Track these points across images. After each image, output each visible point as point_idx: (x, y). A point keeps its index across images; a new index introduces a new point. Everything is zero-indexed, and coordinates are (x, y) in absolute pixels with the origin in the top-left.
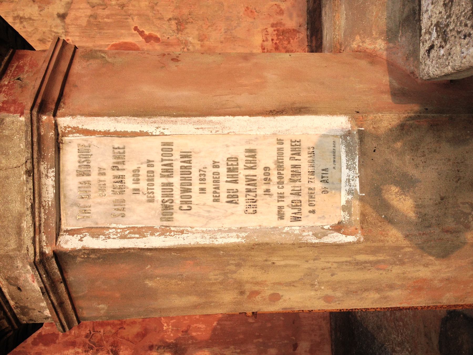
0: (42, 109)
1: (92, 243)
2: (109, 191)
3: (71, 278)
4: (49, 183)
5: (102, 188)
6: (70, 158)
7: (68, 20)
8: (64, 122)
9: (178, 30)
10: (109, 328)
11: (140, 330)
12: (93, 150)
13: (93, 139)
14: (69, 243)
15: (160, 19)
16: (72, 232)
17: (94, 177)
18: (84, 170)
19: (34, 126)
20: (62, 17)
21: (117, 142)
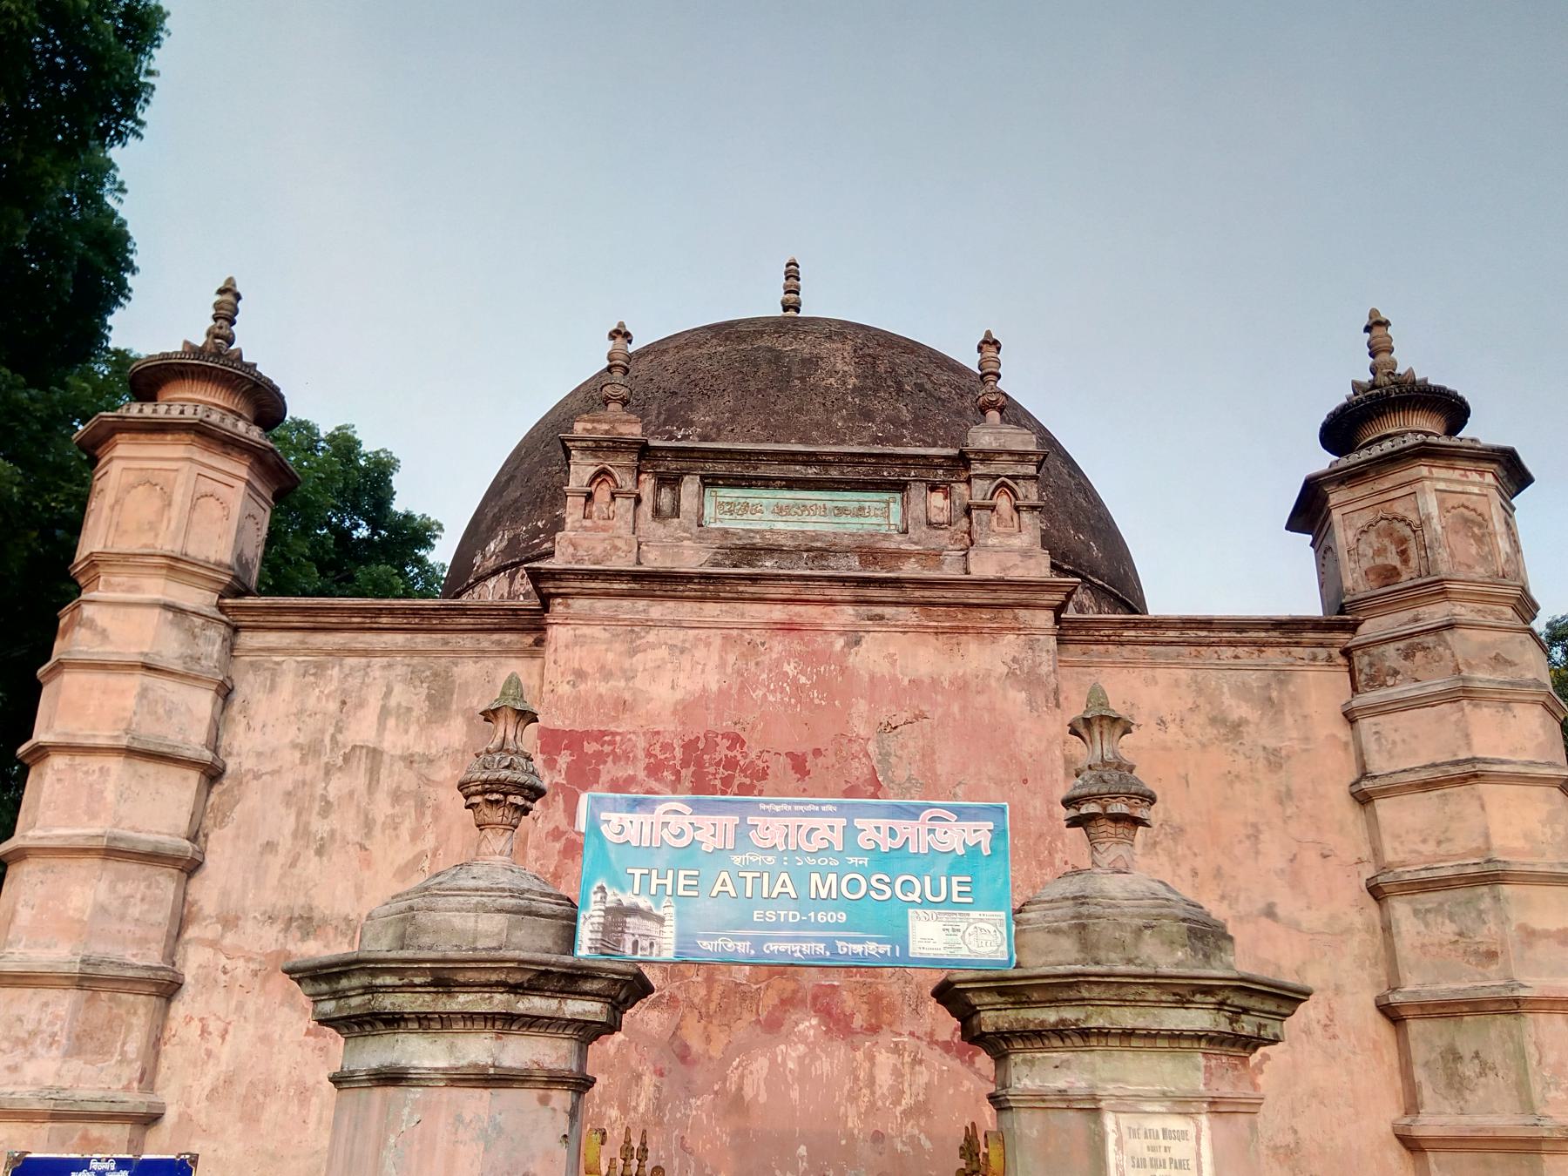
0: (1211, 1103)
1: (1111, 1139)
2: (1152, 1155)
3: (1070, 1113)
4: (1156, 1107)
5: (1152, 1149)
6: (1176, 1123)
7: (1265, 922)
8: (1204, 1120)
9: (1276, 1148)
10: (703, 992)
11: (694, 1050)
12: (1184, 1142)
13: (1193, 1143)
14: (1109, 1121)
15: (1293, 1109)
16: (1117, 1124)
17: (1163, 1143)
18: (1166, 1133)
19: (1200, 1098)
20: (1270, 912)
21: (1193, 1163)
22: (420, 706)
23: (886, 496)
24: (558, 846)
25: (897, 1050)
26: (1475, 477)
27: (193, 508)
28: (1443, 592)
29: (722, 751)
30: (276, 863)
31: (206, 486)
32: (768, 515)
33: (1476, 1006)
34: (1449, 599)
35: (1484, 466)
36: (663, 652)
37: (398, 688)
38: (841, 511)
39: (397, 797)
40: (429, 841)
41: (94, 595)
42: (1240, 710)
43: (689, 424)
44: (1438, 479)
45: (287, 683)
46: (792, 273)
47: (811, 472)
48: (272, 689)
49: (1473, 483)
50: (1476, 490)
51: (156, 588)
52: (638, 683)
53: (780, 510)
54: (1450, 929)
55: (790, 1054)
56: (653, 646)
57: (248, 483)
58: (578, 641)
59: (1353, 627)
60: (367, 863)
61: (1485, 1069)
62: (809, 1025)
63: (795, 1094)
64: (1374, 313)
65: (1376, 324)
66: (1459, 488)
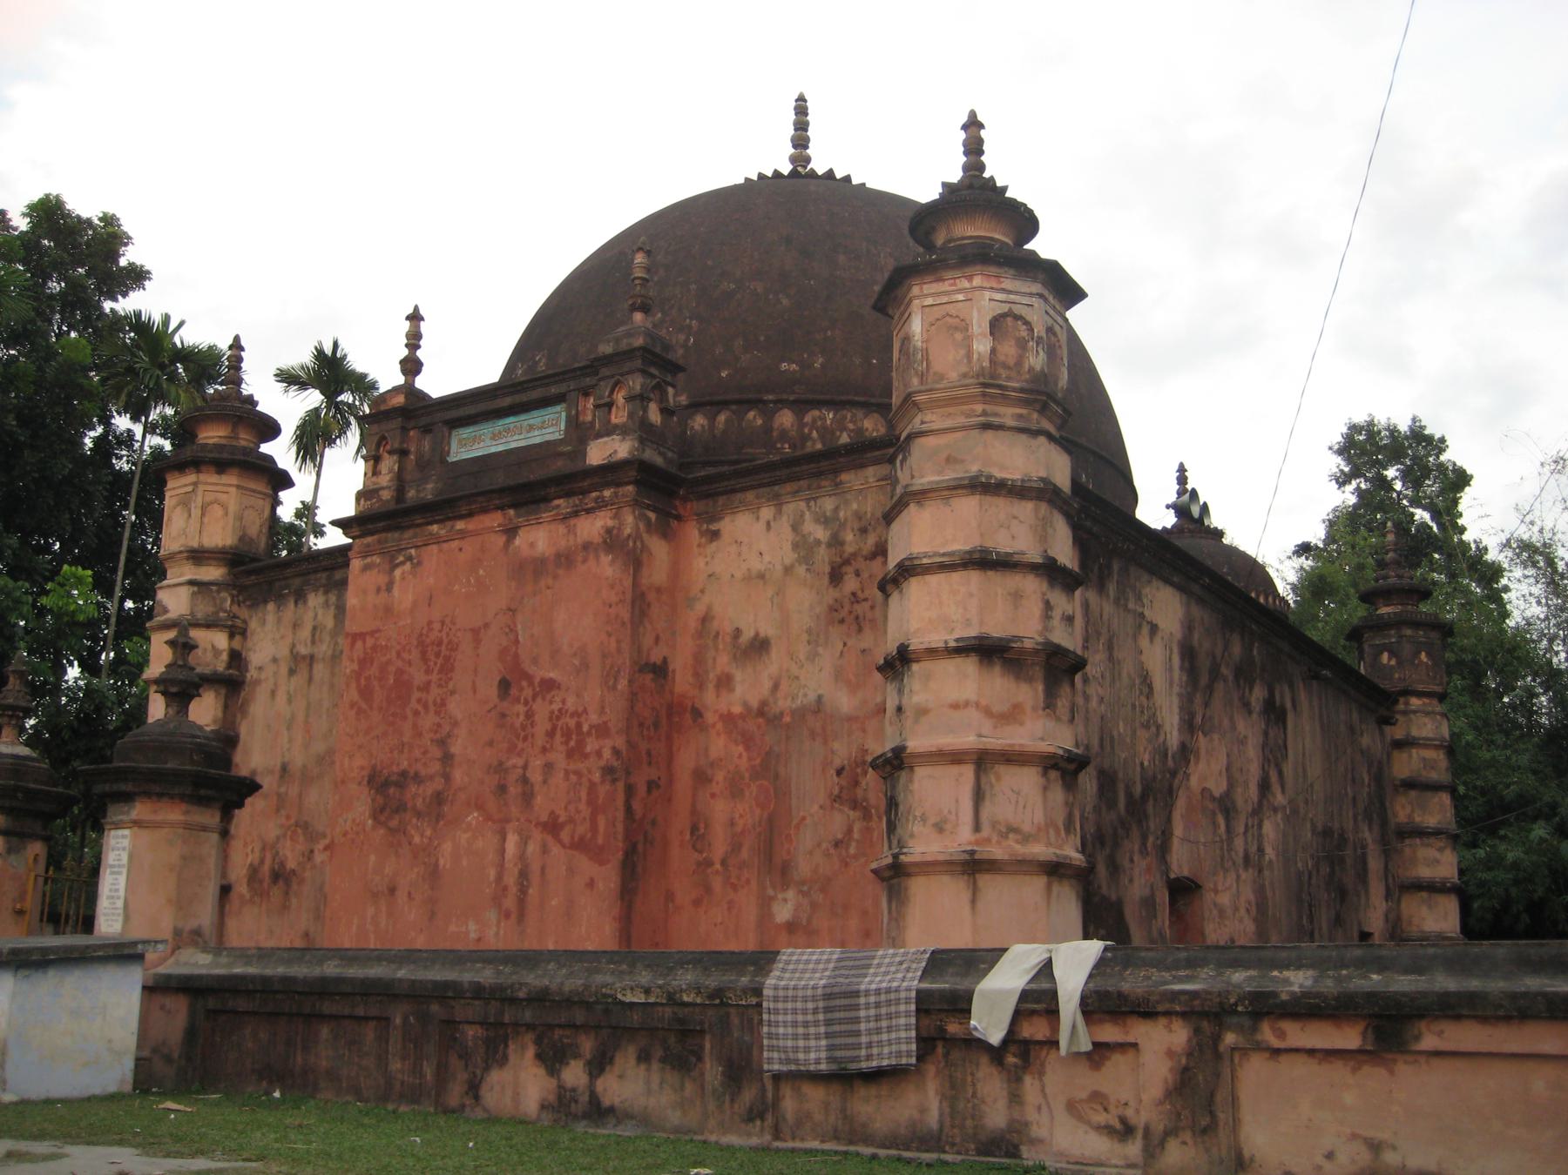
22: (330, 623)
23: (558, 408)
24: (353, 713)
26: (965, 284)
27: (203, 514)
28: (915, 404)
29: (434, 635)
31: (210, 497)
32: (488, 442)
34: (920, 410)
35: (968, 271)
36: (408, 566)
37: (320, 612)
38: (531, 428)
41: (165, 583)
44: (927, 296)
45: (271, 618)
46: (801, 108)
47: (507, 401)
48: (263, 622)
49: (959, 291)
50: (961, 297)
51: (189, 572)
52: (396, 592)
53: (493, 438)
56: (402, 563)
57: (238, 487)
58: (366, 568)
63: (465, 863)
64: (973, 115)
65: (973, 125)
66: (945, 299)
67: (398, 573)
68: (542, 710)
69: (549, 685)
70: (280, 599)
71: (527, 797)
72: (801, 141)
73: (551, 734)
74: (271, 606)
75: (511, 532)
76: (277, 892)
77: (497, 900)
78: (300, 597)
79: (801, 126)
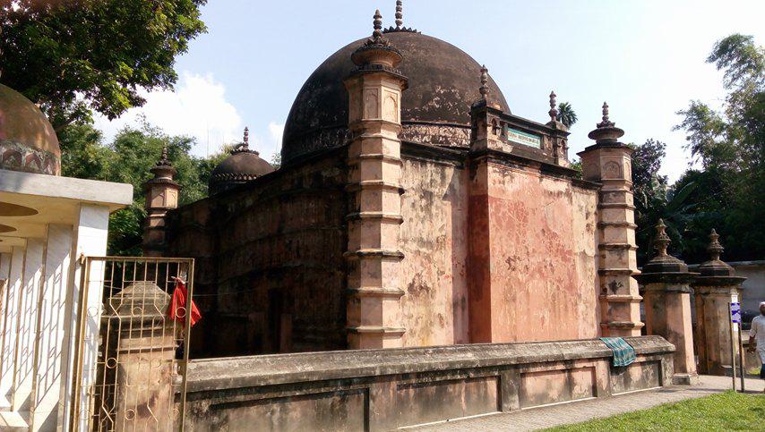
22: (439, 181)
25: (550, 281)
30: (413, 224)
33: (621, 273)
36: (509, 177)
39: (437, 208)
40: (445, 222)
42: (583, 204)
43: (454, 88)
52: (506, 184)
54: (618, 257)
55: (535, 281)
58: (495, 171)
59: (601, 187)
60: (432, 226)
61: (621, 286)
62: (538, 275)
65: (605, 106)
67: (508, 178)
68: (555, 242)
69: (555, 235)
70: (413, 160)
71: (553, 271)
72: (398, 16)
73: (557, 251)
74: (408, 162)
75: (541, 178)
76: (423, 294)
77: (546, 305)
78: (423, 163)
79: (398, 9)
